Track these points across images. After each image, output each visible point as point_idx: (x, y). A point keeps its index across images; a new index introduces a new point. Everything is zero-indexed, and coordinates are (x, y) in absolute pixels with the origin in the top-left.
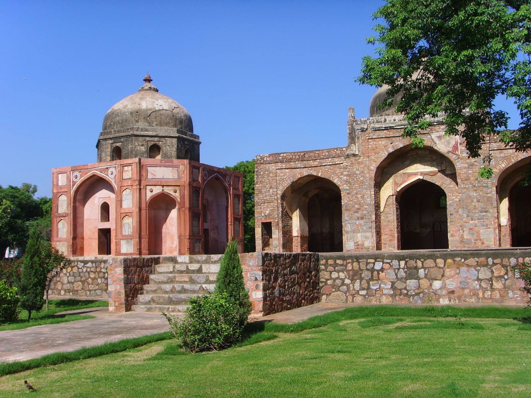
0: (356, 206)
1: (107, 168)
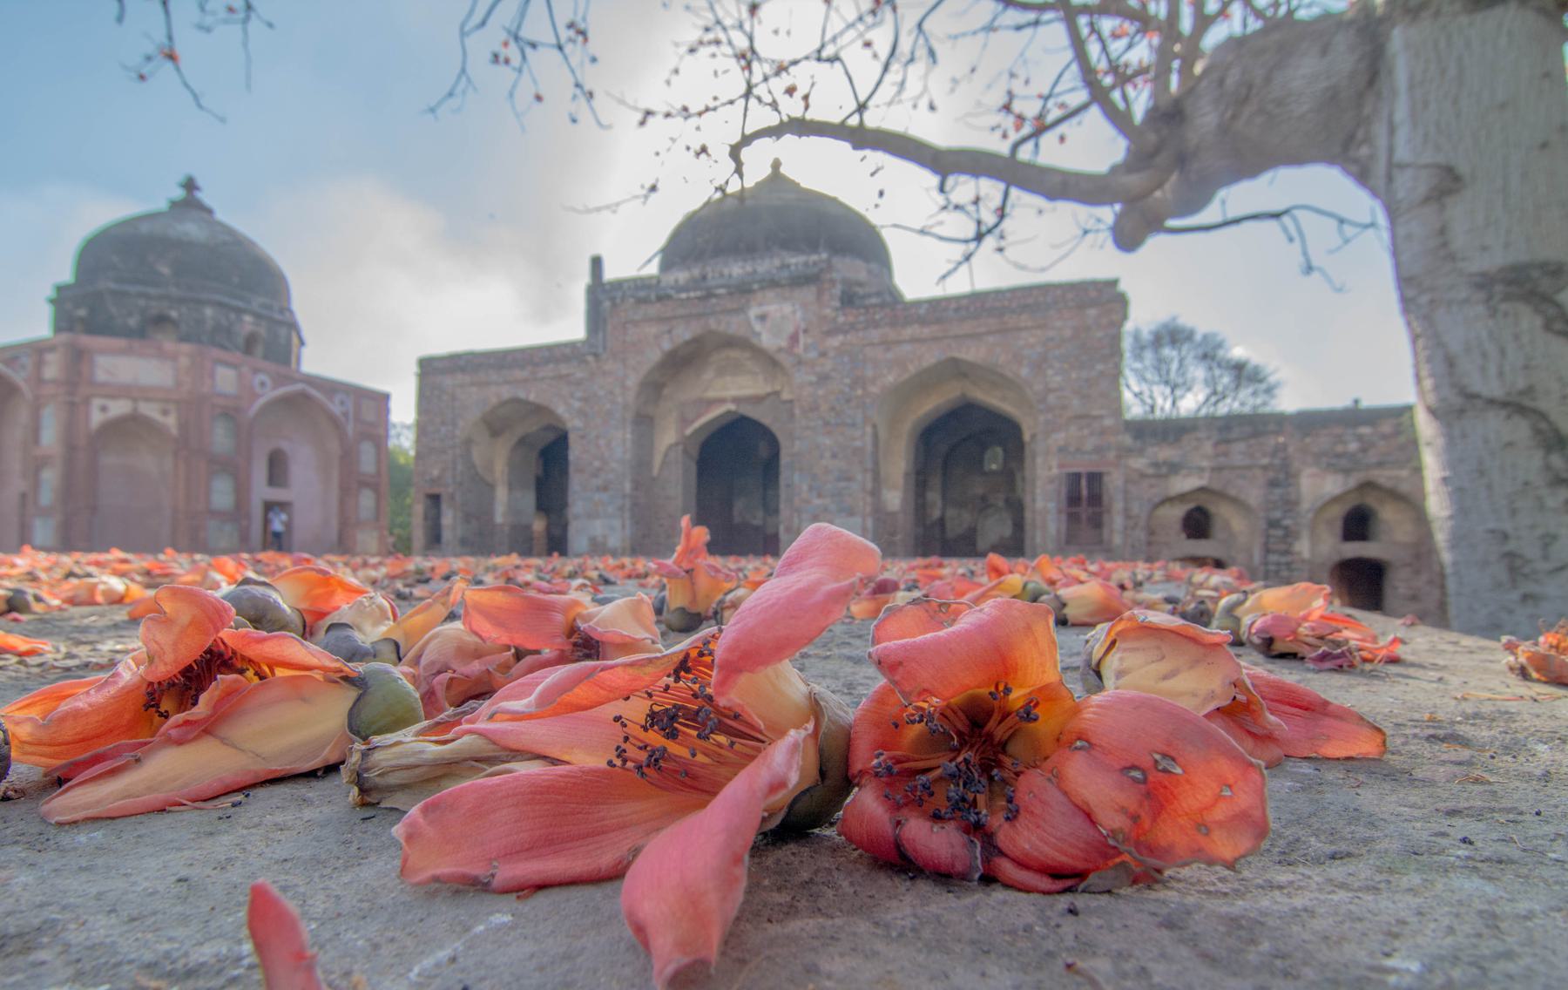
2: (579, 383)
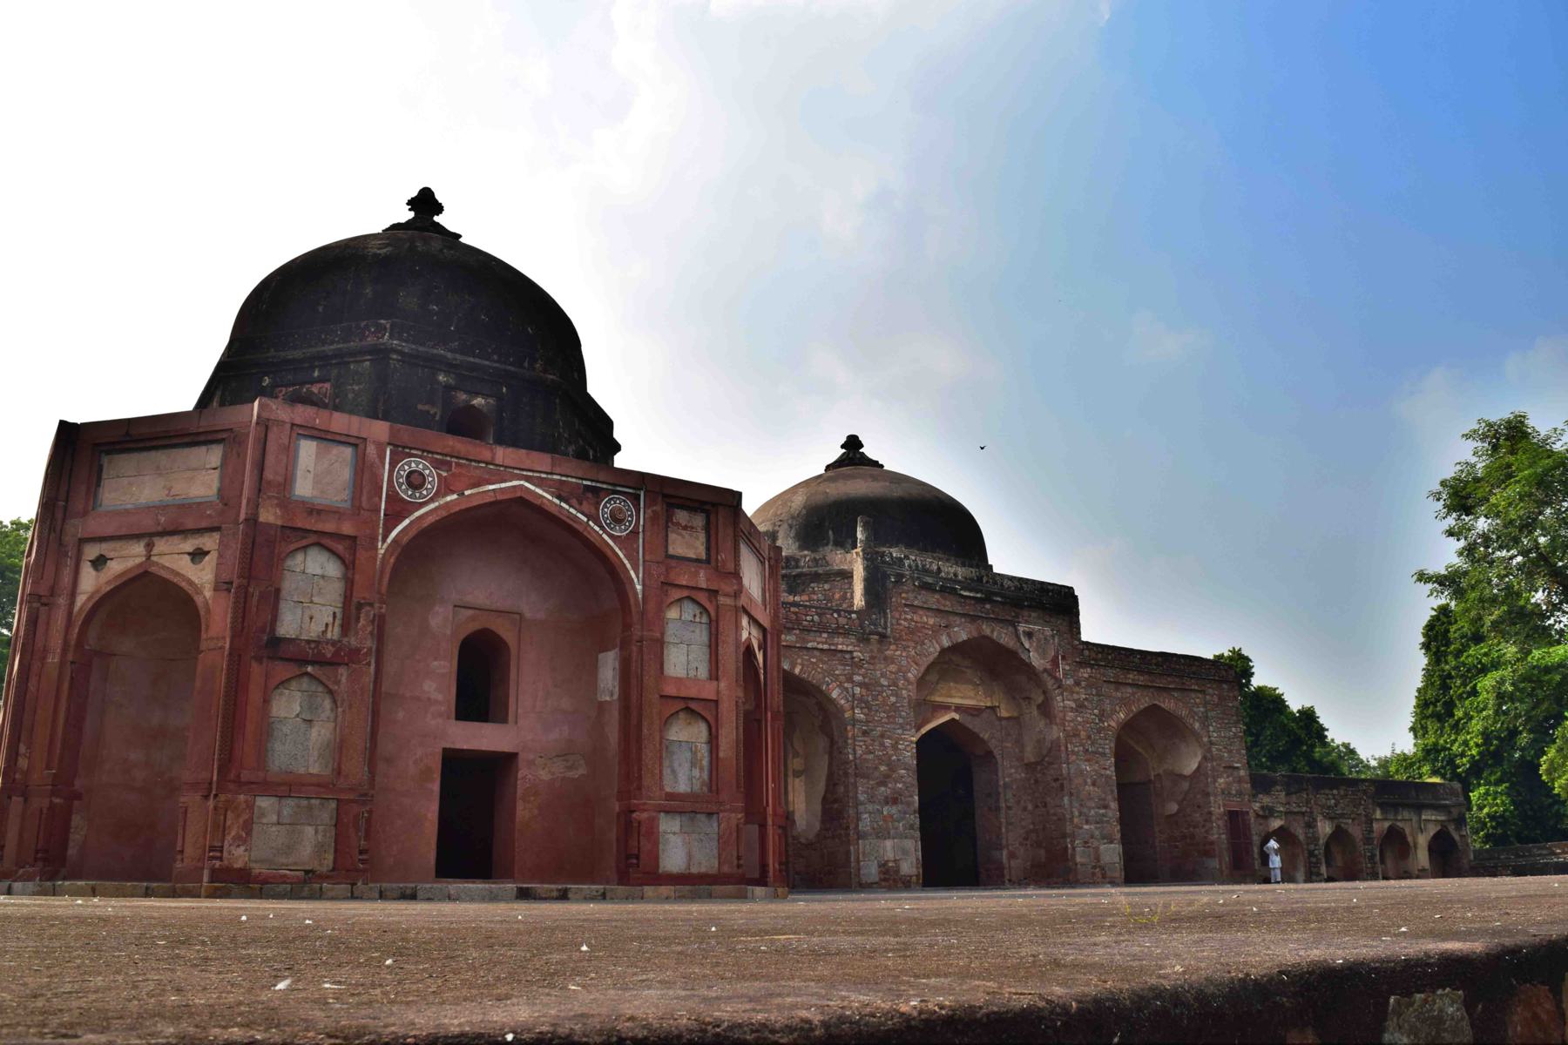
0: (883, 768)
2: (856, 665)
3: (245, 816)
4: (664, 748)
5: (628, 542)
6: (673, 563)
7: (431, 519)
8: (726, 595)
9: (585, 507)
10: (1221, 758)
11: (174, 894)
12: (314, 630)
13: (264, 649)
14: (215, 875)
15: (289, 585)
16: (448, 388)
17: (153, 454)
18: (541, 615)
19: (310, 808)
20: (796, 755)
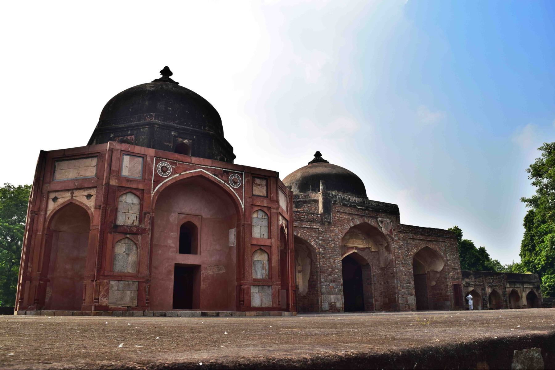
0: (330, 270)
1: (227, 172)
2: (320, 233)
3: (106, 288)
4: (252, 263)
5: (239, 190)
6: (255, 198)
7: (170, 183)
8: (273, 209)
9: (224, 178)
10: (451, 265)
11: (82, 315)
12: (129, 222)
13: (112, 228)
14: (96, 308)
15: (121, 206)
16: (175, 137)
17: (73, 161)
18: (209, 216)
19: (129, 285)
20: (299, 265)
